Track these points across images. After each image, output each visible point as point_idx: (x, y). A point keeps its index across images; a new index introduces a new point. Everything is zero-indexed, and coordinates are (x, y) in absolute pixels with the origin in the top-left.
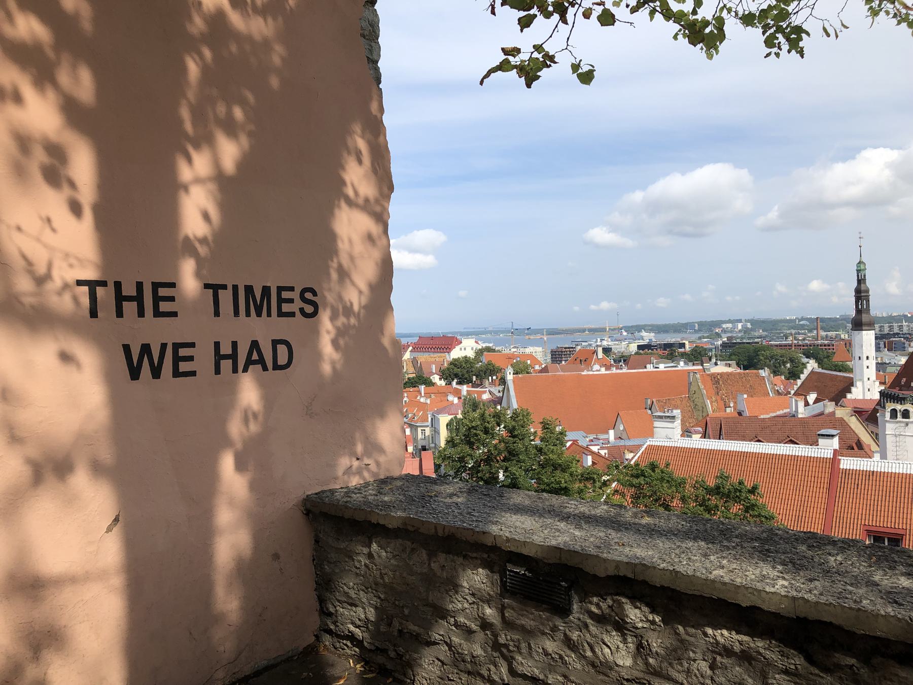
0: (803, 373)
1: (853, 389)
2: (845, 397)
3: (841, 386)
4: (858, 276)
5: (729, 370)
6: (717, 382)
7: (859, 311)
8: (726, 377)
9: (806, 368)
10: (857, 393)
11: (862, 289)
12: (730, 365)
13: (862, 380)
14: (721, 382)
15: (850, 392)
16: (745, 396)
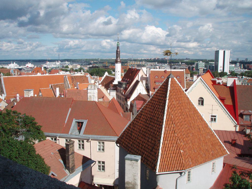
0: (103, 76)
1: (114, 81)
2: (112, 83)
3: (110, 80)
4: (117, 47)
5: (82, 75)
6: (73, 79)
7: (117, 57)
8: (76, 77)
9: (104, 74)
10: (116, 82)
11: (118, 51)
12: (81, 73)
13: (117, 78)
14: (74, 79)
15: (114, 82)
16: (79, 83)
